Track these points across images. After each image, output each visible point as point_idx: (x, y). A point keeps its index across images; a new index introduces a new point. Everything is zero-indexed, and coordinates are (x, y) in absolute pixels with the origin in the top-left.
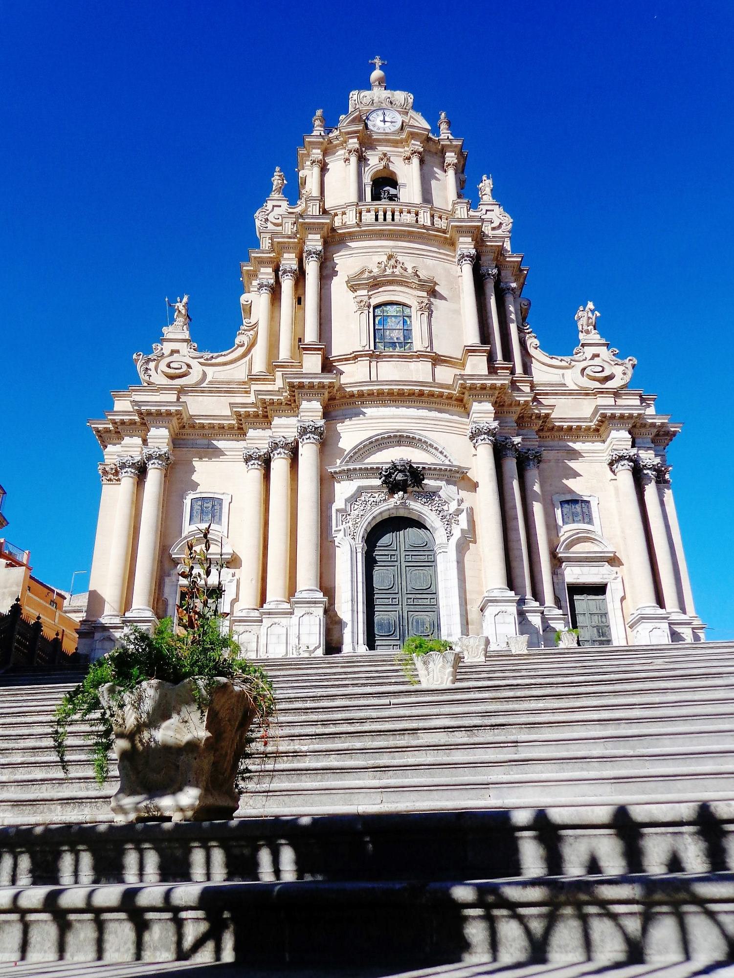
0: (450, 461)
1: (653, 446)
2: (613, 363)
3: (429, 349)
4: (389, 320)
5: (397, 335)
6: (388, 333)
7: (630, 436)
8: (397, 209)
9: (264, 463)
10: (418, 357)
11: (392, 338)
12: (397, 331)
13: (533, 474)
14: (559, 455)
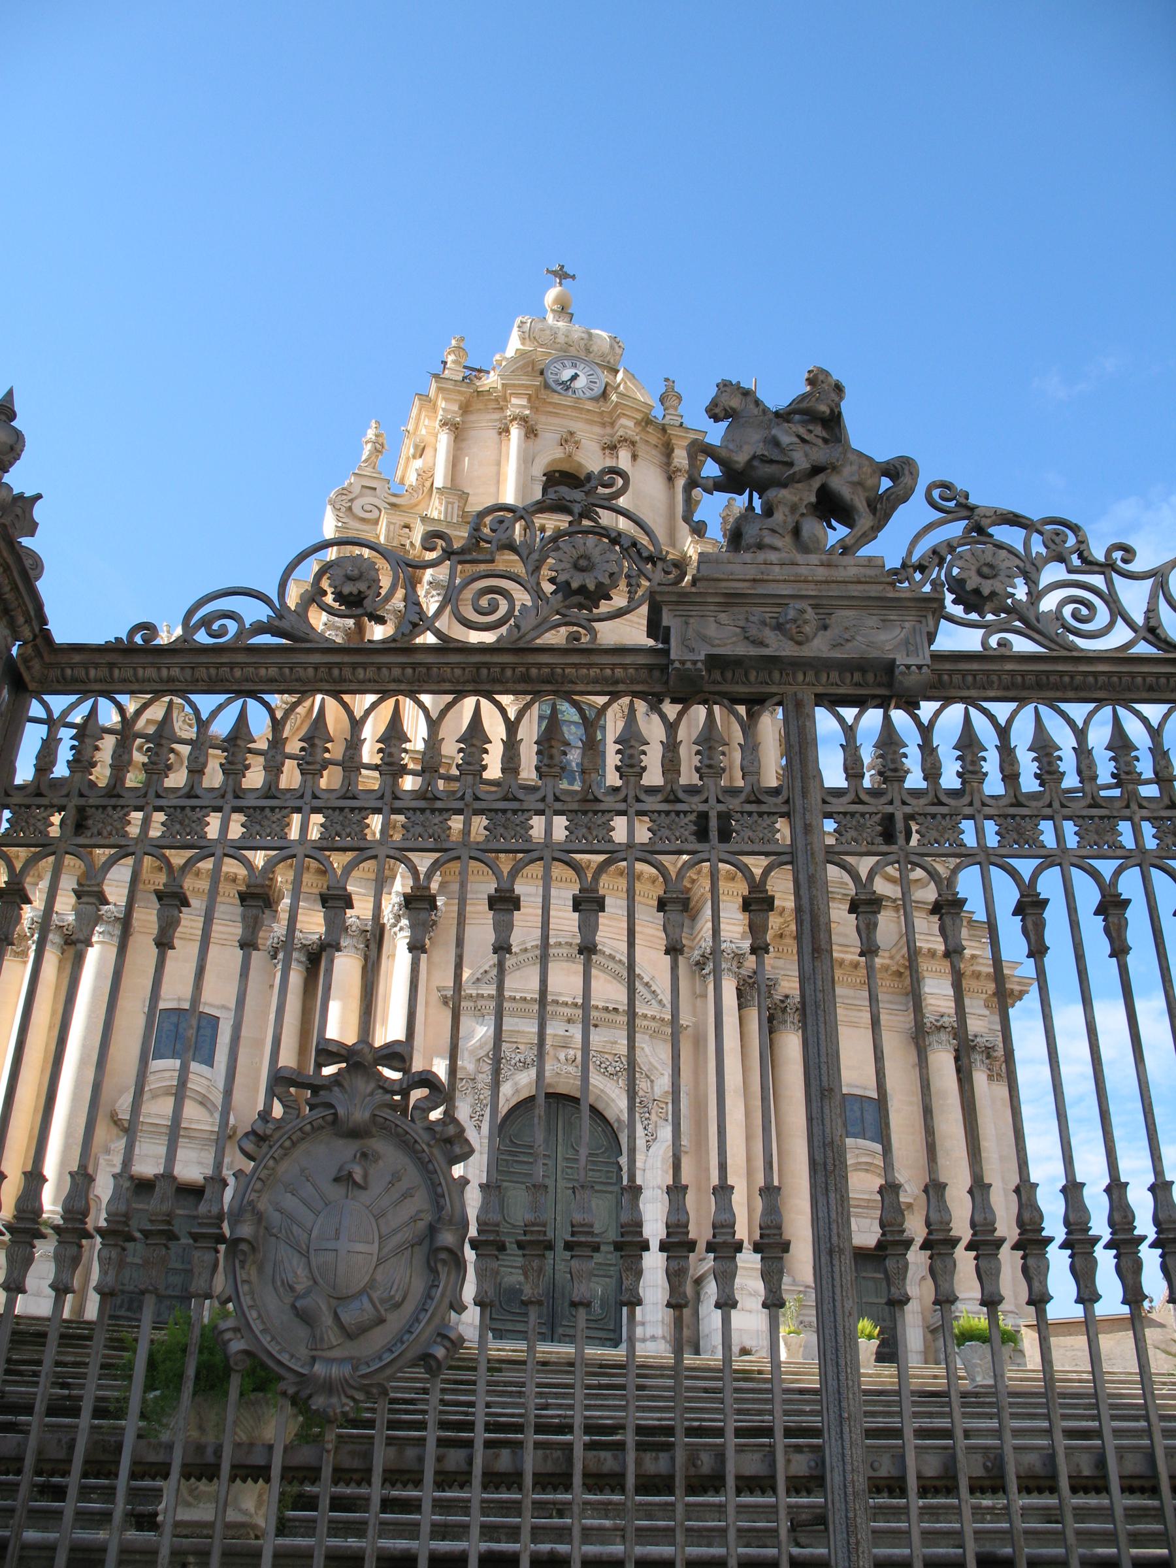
9: (309, 959)
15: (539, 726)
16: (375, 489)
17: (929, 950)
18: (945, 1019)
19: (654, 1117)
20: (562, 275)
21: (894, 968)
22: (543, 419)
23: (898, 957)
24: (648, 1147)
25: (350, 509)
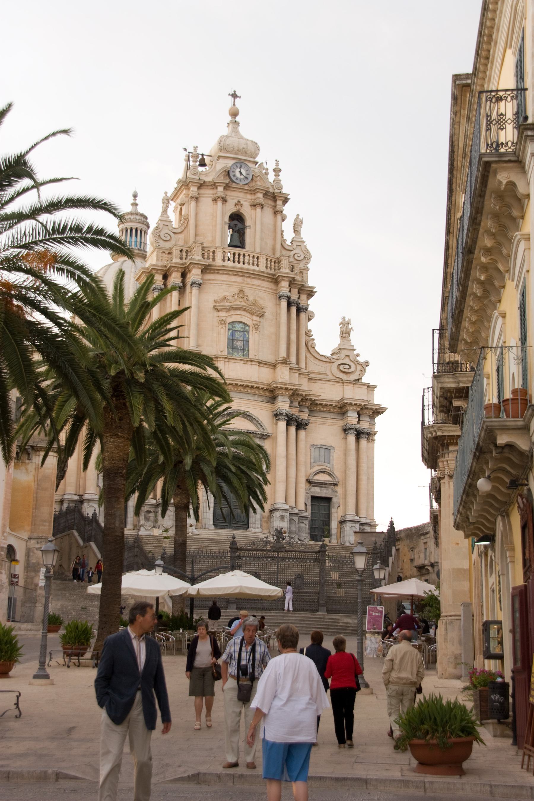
1: (369, 420)
2: (356, 363)
3: (257, 358)
4: (236, 333)
5: (239, 344)
6: (235, 342)
8: (246, 255)
10: (251, 361)
11: (237, 346)
13: (302, 433)
14: (318, 420)
18: (353, 426)
20: (234, 96)
22: (228, 193)
25: (159, 235)
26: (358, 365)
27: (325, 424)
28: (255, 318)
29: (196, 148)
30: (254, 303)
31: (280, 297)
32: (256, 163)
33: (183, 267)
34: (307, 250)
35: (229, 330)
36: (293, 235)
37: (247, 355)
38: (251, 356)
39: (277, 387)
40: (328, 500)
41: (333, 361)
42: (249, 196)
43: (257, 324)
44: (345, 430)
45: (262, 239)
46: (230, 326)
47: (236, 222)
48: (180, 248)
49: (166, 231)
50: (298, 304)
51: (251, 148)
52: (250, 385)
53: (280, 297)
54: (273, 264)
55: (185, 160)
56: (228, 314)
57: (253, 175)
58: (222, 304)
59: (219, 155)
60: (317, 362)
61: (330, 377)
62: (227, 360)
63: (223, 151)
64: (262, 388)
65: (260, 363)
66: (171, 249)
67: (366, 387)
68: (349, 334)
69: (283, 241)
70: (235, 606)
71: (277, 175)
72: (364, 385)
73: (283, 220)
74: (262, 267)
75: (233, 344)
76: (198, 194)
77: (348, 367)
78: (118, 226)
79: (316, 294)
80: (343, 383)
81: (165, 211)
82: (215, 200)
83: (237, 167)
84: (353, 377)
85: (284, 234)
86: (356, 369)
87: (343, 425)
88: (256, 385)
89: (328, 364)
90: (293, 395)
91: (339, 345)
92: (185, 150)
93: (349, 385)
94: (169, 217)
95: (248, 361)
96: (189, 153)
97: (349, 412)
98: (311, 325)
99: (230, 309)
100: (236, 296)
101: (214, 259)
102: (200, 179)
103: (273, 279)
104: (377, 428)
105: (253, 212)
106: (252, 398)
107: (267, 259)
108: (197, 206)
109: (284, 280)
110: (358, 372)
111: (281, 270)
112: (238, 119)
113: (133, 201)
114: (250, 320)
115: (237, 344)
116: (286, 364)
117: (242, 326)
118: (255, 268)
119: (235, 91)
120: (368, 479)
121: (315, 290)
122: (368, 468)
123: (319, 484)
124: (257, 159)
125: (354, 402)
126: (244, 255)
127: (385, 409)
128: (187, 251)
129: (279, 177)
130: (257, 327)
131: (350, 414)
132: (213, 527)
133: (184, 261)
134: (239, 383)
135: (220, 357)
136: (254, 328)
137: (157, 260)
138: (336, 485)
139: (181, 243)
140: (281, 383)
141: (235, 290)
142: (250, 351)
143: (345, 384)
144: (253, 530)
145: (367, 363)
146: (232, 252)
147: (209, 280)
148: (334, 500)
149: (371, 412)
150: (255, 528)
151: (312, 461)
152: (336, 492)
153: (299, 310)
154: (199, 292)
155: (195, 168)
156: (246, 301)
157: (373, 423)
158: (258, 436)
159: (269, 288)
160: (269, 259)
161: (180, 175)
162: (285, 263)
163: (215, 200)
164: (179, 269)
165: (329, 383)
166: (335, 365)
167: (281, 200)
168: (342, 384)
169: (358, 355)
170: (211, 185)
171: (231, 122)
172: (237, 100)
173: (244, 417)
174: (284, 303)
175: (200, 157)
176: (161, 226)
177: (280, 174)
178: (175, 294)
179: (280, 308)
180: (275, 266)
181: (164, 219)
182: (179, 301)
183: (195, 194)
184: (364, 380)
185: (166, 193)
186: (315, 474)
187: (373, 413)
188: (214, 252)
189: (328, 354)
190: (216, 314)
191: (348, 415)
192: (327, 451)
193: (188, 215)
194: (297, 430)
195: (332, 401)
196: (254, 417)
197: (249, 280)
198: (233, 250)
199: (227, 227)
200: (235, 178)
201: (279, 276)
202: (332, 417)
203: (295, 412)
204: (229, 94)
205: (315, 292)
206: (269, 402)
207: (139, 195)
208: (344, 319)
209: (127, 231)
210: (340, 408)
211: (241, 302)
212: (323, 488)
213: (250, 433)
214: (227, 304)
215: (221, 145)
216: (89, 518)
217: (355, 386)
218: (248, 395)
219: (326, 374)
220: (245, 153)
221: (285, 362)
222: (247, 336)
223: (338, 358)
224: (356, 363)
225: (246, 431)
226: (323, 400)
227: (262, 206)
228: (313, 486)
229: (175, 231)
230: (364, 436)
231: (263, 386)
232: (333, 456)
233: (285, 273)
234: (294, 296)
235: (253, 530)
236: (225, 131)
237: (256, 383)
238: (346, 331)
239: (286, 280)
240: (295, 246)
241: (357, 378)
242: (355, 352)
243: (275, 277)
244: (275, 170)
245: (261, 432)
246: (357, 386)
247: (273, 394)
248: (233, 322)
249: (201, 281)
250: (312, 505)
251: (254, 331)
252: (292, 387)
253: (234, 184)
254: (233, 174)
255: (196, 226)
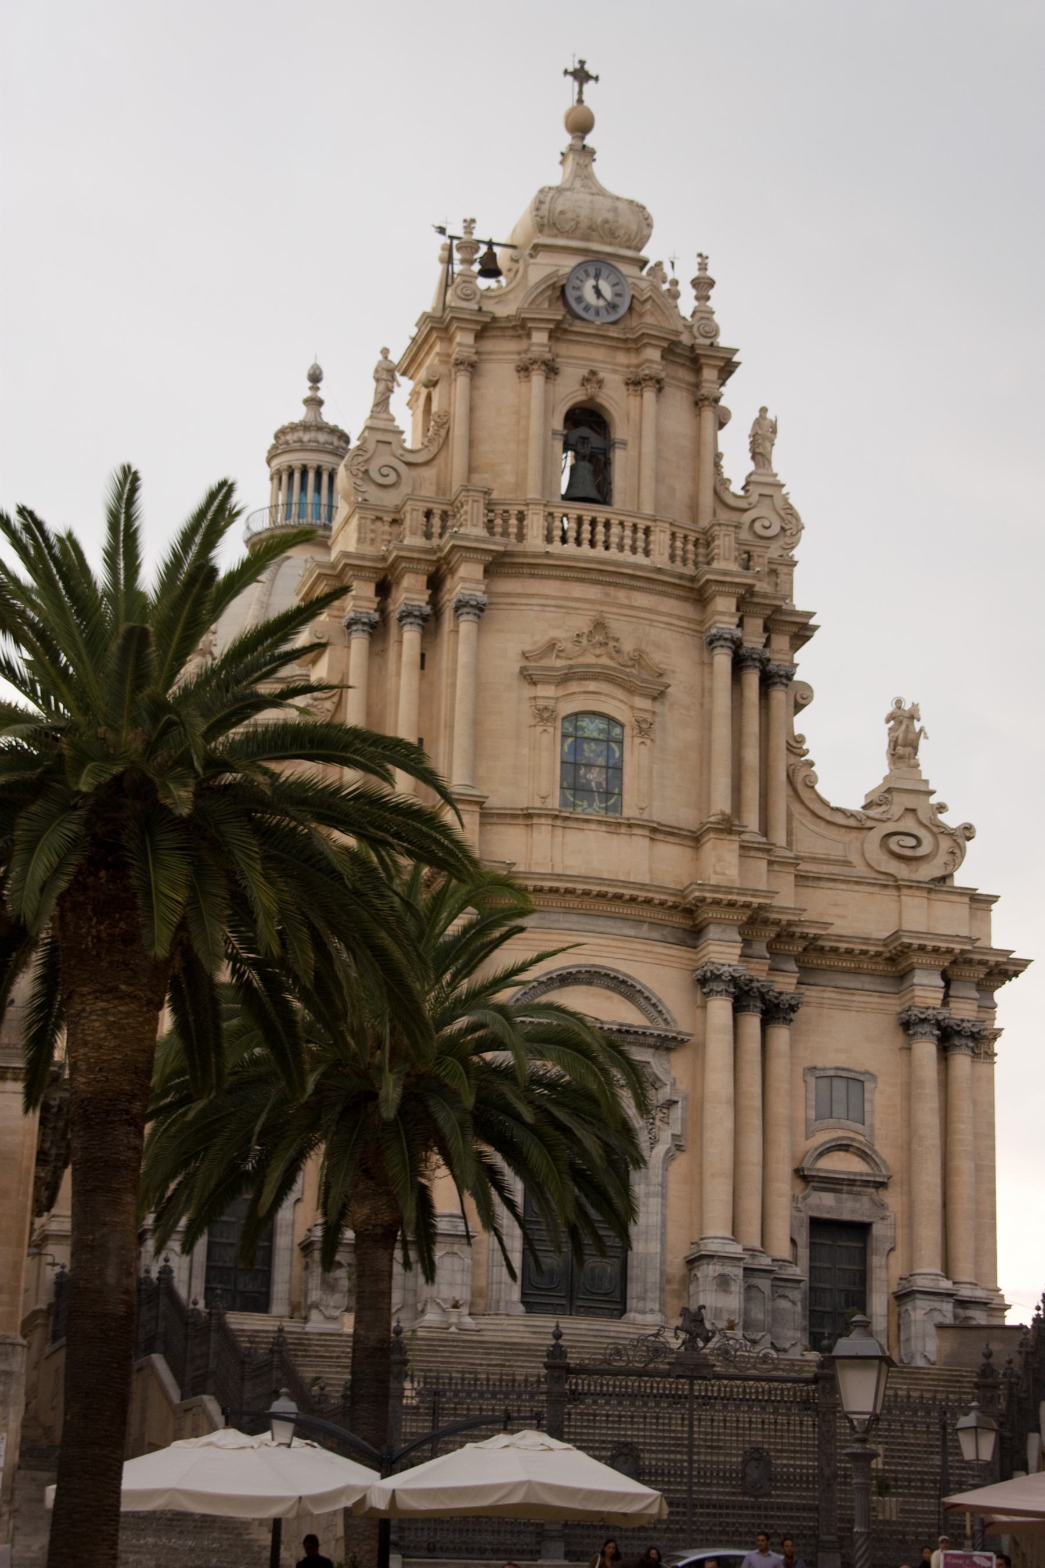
0: (665, 1020)
1: (977, 995)
2: (935, 829)
3: (645, 816)
4: (586, 746)
5: (594, 777)
6: (582, 771)
7: (942, 984)
8: (614, 522)
10: (630, 826)
11: (589, 781)
12: (597, 769)
13: (781, 1035)
14: (826, 995)
15: (562, 746)
16: (390, 443)
17: (920, 945)
18: (930, 1012)
19: (658, 1123)
20: (581, 75)
21: (888, 955)
22: (563, 349)
23: (891, 947)
24: (652, 1148)
25: (366, 472)
26: (941, 838)
27: (846, 1008)
28: (640, 702)
29: (470, 224)
30: (638, 659)
31: (711, 642)
32: (643, 263)
33: (434, 558)
34: (791, 508)
35: (565, 736)
36: (751, 466)
37: (618, 807)
38: (629, 810)
39: (703, 900)
40: (861, 1230)
41: (869, 824)
42: (622, 358)
43: (645, 721)
44: (908, 1025)
45: (659, 479)
46: (567, 725)
47: (584, 431)
48: (423, 507)
49: (384, 458)
50: (764, 662)
51: (628, 221)
52: (627, 892)
53: (712, 642)
54: (690, 547)
55: (442, 261)
56: (561, 692)
57: (633, 297)
58: (545, 663)
59: (536, 241)
60: (821, 828)
61: (861, 870)
62: (559, 822)
63: (546, 229)
64: (662, 903)
65: (654, 830)
66: (398, 510)
67: (966, 900)
68: (915, 748)
69: (721, 484)
70: (560, 1547)
71: (703, 297)
72: (961, 894)
73: (721, 425)
74: (660, 557)
75: (576, 776)
76: (477, 353)
77: (913, 842)
78: (269, 462)
79: (817, 633)
80: (898, 888)
81: (382, 402)
82: (524, 370)
83: (588, 275)
84: (927, 872)
85: (723, 463)
86: (937, 846)
87: (899, 1009)
88: (642, 895)
89: (854, 835)
90: (752, 921)
91: (886, 778)
92: (442, 230)
93: (917, 893)
94: (393, 420)
95: (619, 824)
96: (452, 238)
97: (917, 972)
98: (802, 723)
99: (566, 678)
100: (584, 641)
101: (521, 537)
102: (480, 309)
103: (691, 589)
104: (1001, 1020)
105: (634, 401)
106: (632, 932)
107: (673, 535)
108: (473, 387)
109: (722, 594)
110: (942, 858)
111: (715, 565)
112: (590, 140)
113: (308, 394)
114: (624, 707)
115: (590, 776)
116: (730, 832)
117: (601, 724)
118: (640, 558)
119: (582, 63)
120: (978, 1168)
121: (812, 622)
122: (976, 1135)
123: (832, 1183)
124: (645, 253)
125: (930, 944)
126: (607, 525)
127: (1024, 964)
128: (444, 516)
129: (709, 303)
130: (644, 729)
131: (919, 977)
132: (521, 1308)
133: (435, 542)
134: (596, 889)
135: (540, 816)
136: (636, 731)
137: (360, 540)
138: (881, 1185)
139: (428, 491)
140: (716, 888)
141: (582, 623)
142: (626, 797)
143: (905, 891)
144: (639, 1318)
145: (968, 832)
146: (574, 514)
147: (508, 595)
148: (878, 1230)
149: (981, 973)
150: (644, 1313)
151: (812, 1114)
152: (883, 1206)
153: (767, 681)
154: (480, 630)
155: (468, 279)
156: (614, 654)
157: (989, 1004)
158: (651, 1041)
159: (679, 618)
160: (680, 535)
161: (427, 301)
162: (724, 543)
163: (524, 370)
164: (422, 566)
165: (857, 888)
166: (873, 839)
167: (715, 366)
168: (894, 892)
169: (941, 808)
170: (514, 327)
171: (571, 148)
172: (589, 87)
173: (608, 988)
174: (723, 660)
175: (483, 249)
176: (371, 446)
177: (712, 293)
178: (411, 636)
179: (711, 673)
180: (696, 555)
181: (381, 424)
182: (423, 656)
183: (469, 354)
184: (962, 878)
185: (385, 352)
186: (821, 1155)
187: (989, 974)
188: (521, 517)
189: (854, 803)
190: (528, 691)
191: (916, 980)
192: (854, 1087)
193: (447, 414)
194: (765, 1024)
195: (866, 940)
196: (639, 987)
197: (621, 595)
198: (576, 509)
199: (559, 445)
200: (583, 305)
201: (708, 581)
202: (867, 987)
203: (758, 971)
204: (566, 72)
205: (815, 628)
206: (681, 943)
207: (326, 375)
208: (899, 703)
209: (291, 476)
210: (892, 960)
211: (598, 656)
212: (845, 1196)
213: (628, 1032)
214: (559, 663)
215: (540, 213)
216: (151, 1280)
217: (933, 896)
218: (620, 924)
219: (847, 863)
220: (610, 234)
221: (728, 826)
222: (617, 754)
223: (884, 817)
224: (935, 829)
225: (615, 1027)
226: (840, 938)
227: (659, 385)
228: (815, 1189)
229: (410, 458)
230: (963, 1041)
231: (663, 897)
232: (872, 1101)
233: (725, 573)
234: (753, 639)
235: (639, 1318)
236: (555, 175)
237: (643, 887)
238: (905, 738)
239: (728, 594)
240: (754, 498)
241: (938, 873)
242: (933, 800)
243: (696, 586)
244: (696, 283)
245: (659, 1029)
246: (941, 896)
247: (694, 919)
248: (576, 715)
249: (484, 599)
250: (812, 1245)
251: (638, 740)
252: (749, 899)
253: (578, 322)
254: (577, 293)
255: (472, 443)
